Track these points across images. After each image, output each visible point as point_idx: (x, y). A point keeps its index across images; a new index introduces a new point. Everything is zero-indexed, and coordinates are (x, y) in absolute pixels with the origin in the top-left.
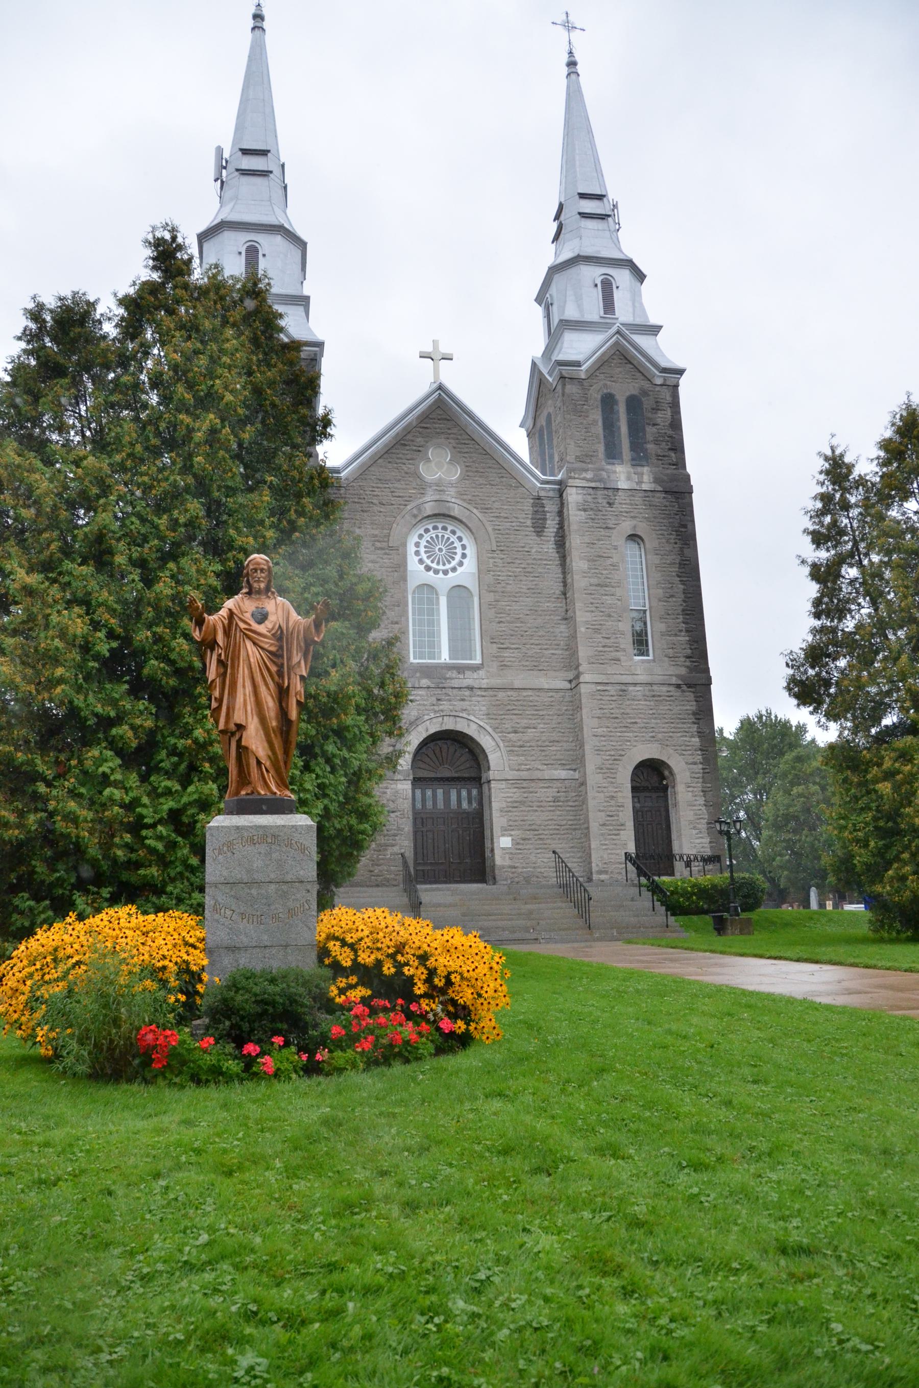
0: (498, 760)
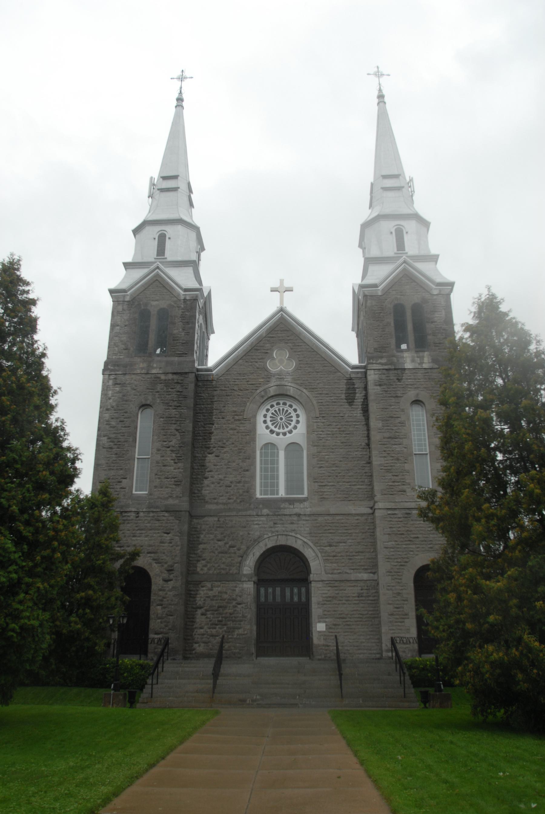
0: (316, 565)
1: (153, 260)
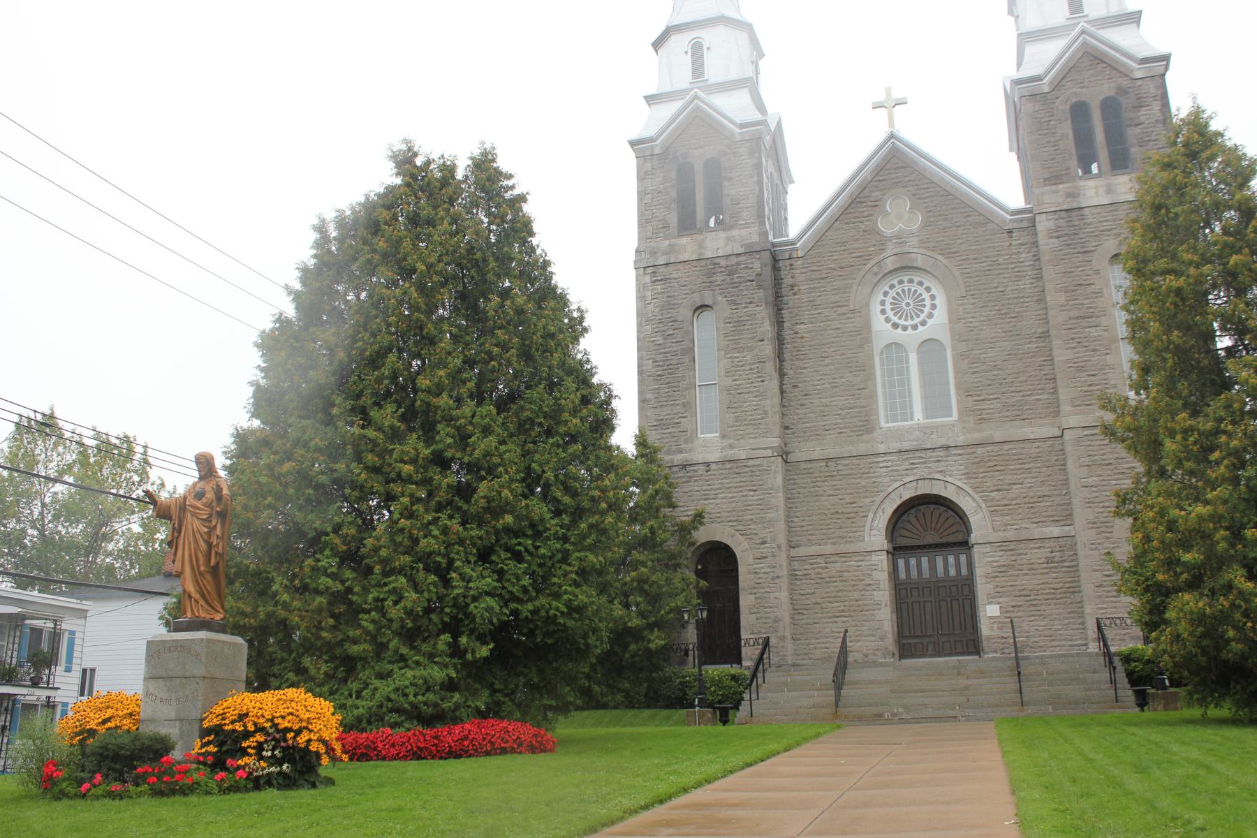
1: (687, 86)
